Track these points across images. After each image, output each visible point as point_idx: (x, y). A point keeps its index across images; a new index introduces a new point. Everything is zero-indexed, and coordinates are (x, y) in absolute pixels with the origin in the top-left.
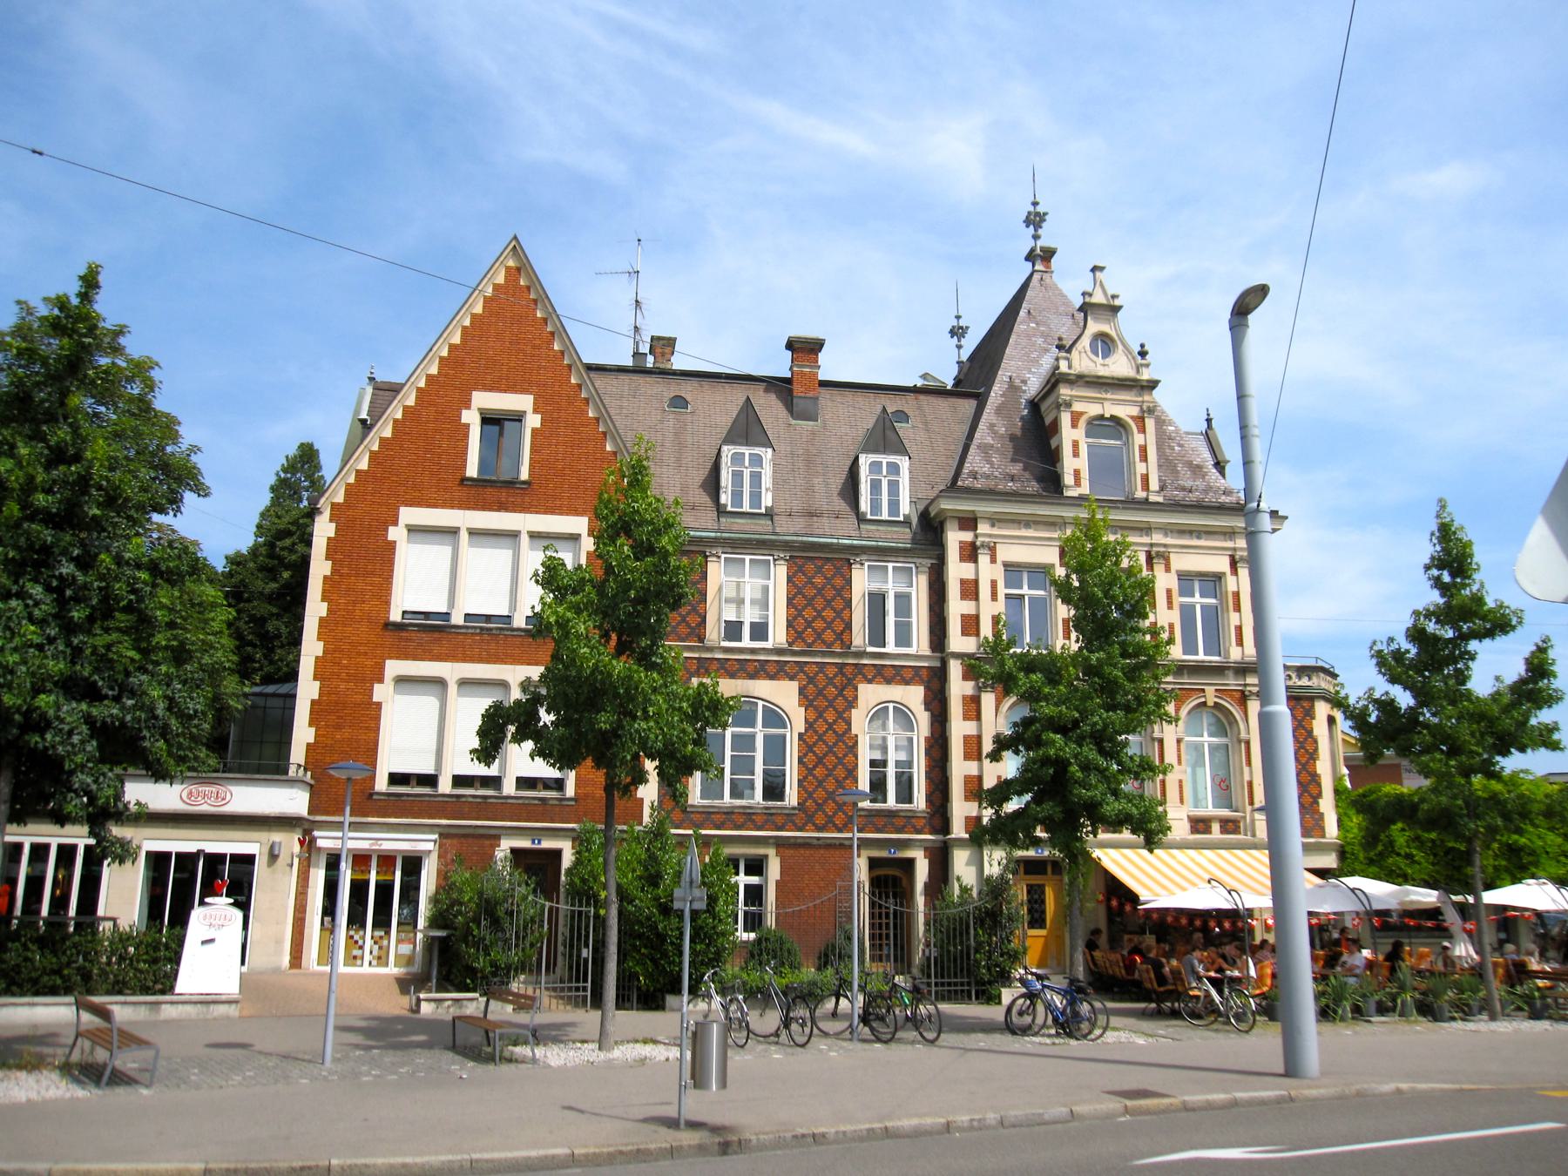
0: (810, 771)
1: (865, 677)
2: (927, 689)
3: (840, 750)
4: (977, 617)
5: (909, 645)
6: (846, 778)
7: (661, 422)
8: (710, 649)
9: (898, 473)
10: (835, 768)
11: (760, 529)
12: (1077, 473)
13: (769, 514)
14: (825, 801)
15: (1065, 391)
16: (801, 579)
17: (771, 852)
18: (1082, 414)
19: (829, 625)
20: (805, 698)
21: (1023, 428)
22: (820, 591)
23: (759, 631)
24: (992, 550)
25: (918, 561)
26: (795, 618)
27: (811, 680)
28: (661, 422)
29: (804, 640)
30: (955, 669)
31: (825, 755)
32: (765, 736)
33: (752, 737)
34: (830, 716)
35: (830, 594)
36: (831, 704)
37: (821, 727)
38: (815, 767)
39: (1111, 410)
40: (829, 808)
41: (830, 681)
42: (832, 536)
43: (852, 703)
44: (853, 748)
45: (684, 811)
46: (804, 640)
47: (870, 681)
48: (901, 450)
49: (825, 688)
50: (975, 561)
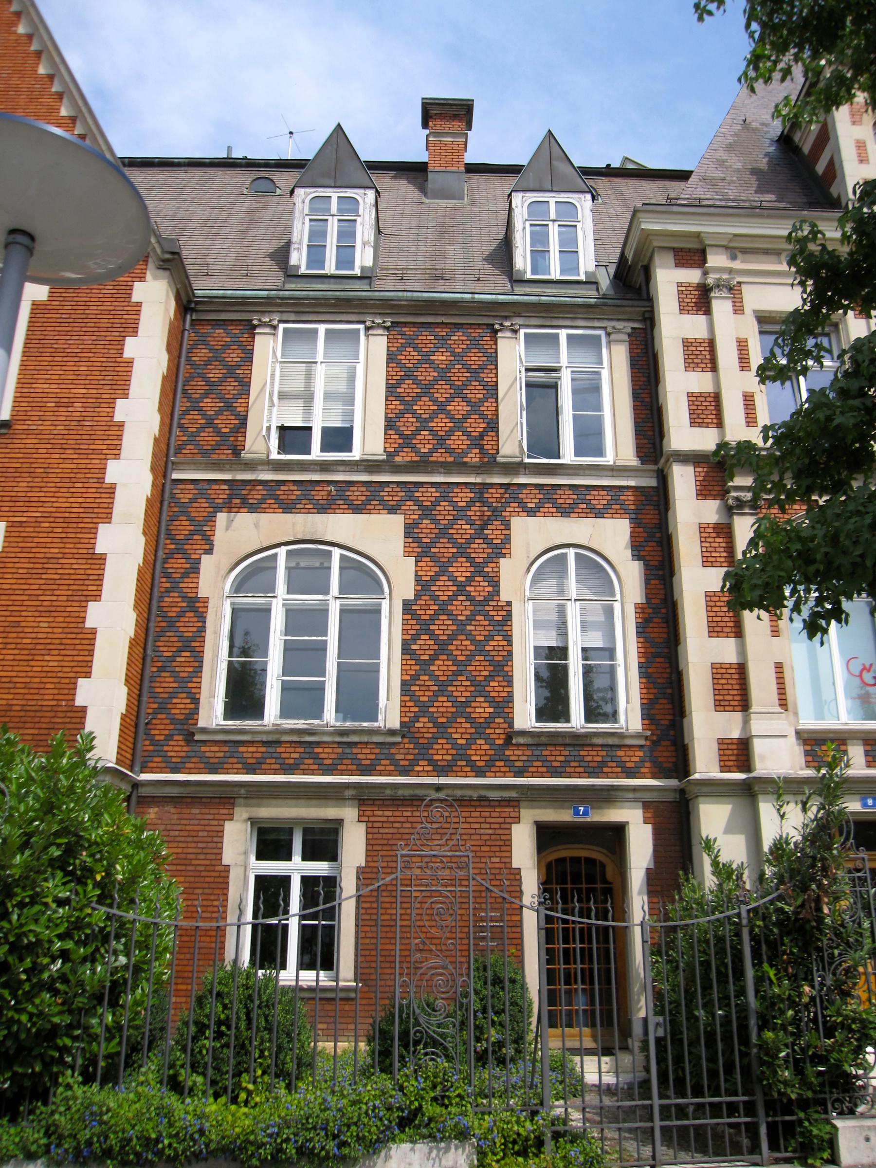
0: (424, 666)
2: (637, 524)
3: (479, 628)
4: (717, 398)
5: (599, 451)
6: (490, 678)
8: (251, 465)
10: (470, 658)
13: (366, 277)
14: (452, 719)
21: (769, 163)
22: (443, 373)
23: (338, 438)
24: (734, 291)
25: (609, 324)
26: (400, 415)
27: (427, 512)
30: (683, 481)
31: (452, 638)
36: (463, 551)
37: (444, 589)
38: (433, 659)
40: (460, 732)
44: (503, 623)
45: (189, 737)
47: (531, 513)
49: (451, 525)
50: (708, 312)
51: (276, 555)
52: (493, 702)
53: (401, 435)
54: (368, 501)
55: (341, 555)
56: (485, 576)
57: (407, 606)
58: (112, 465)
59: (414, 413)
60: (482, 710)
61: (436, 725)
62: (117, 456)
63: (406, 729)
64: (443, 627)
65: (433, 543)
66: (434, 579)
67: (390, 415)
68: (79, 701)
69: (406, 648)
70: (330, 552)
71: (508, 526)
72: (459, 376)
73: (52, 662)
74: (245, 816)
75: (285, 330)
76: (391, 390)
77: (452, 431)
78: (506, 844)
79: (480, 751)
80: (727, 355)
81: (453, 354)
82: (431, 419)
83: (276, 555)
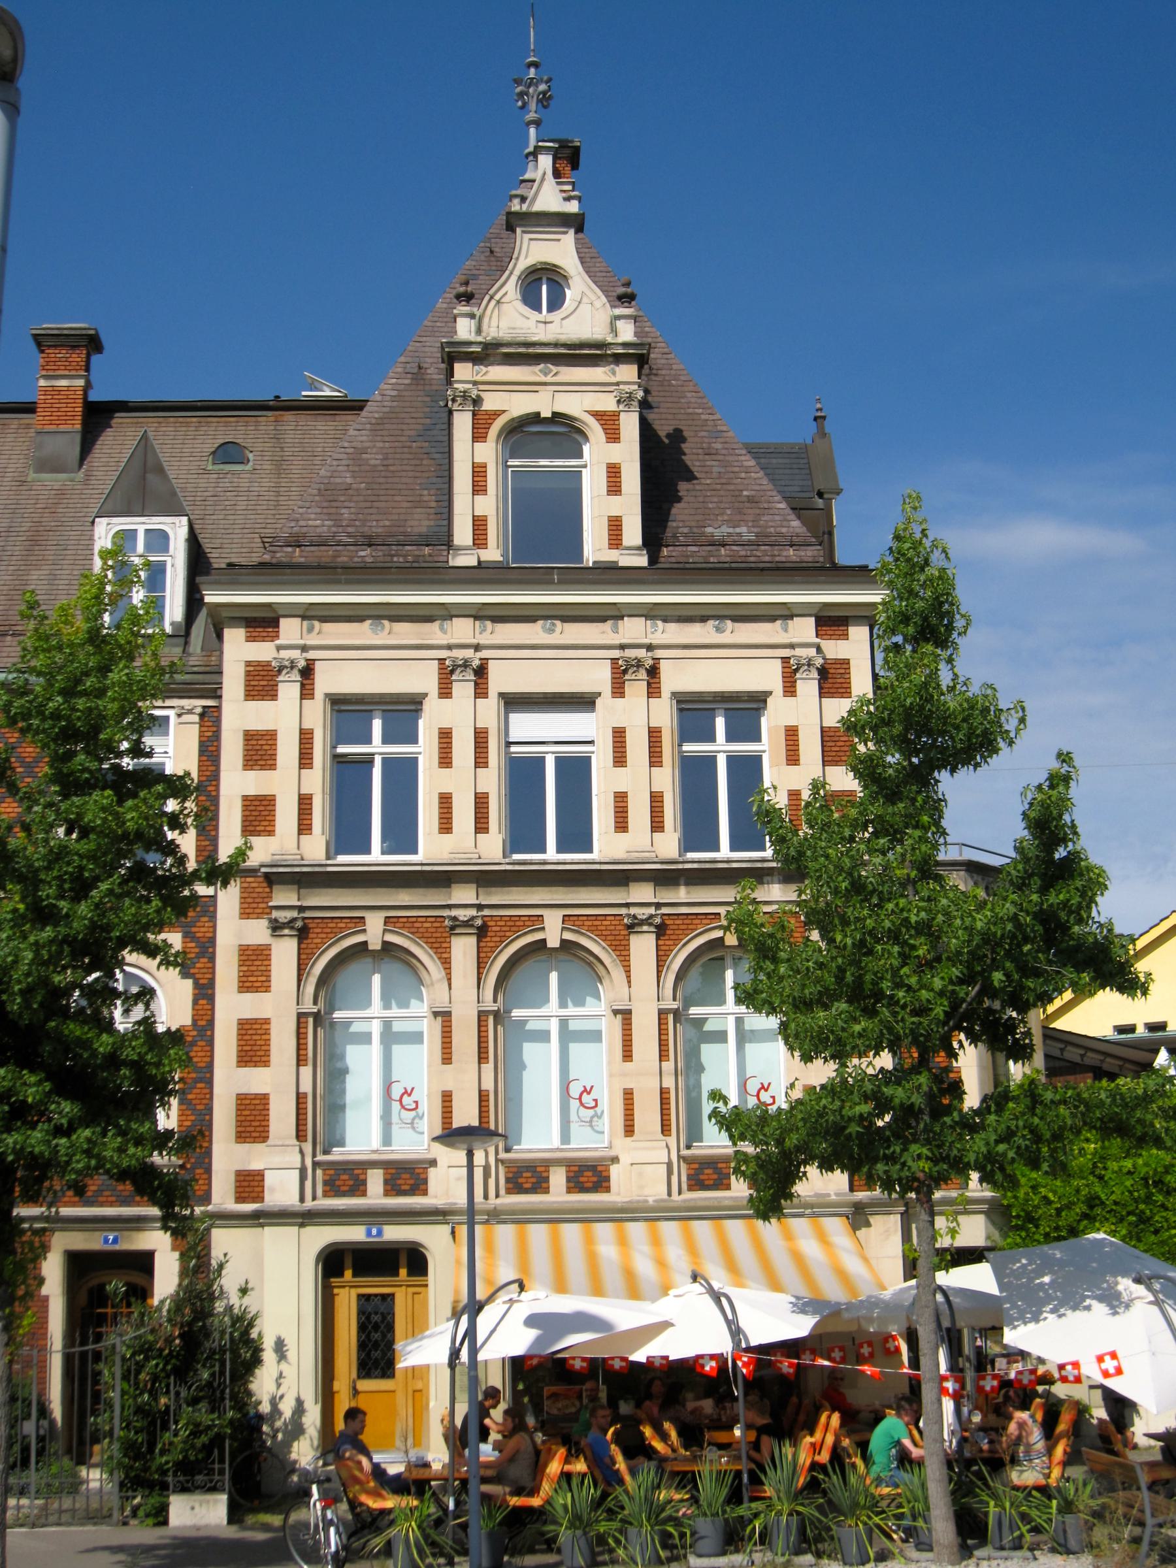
9: (165, 549)
12: (479, 524)
18: (497, 414)
39: (543, 404)
48: (174, 510)
80: (287, 750)
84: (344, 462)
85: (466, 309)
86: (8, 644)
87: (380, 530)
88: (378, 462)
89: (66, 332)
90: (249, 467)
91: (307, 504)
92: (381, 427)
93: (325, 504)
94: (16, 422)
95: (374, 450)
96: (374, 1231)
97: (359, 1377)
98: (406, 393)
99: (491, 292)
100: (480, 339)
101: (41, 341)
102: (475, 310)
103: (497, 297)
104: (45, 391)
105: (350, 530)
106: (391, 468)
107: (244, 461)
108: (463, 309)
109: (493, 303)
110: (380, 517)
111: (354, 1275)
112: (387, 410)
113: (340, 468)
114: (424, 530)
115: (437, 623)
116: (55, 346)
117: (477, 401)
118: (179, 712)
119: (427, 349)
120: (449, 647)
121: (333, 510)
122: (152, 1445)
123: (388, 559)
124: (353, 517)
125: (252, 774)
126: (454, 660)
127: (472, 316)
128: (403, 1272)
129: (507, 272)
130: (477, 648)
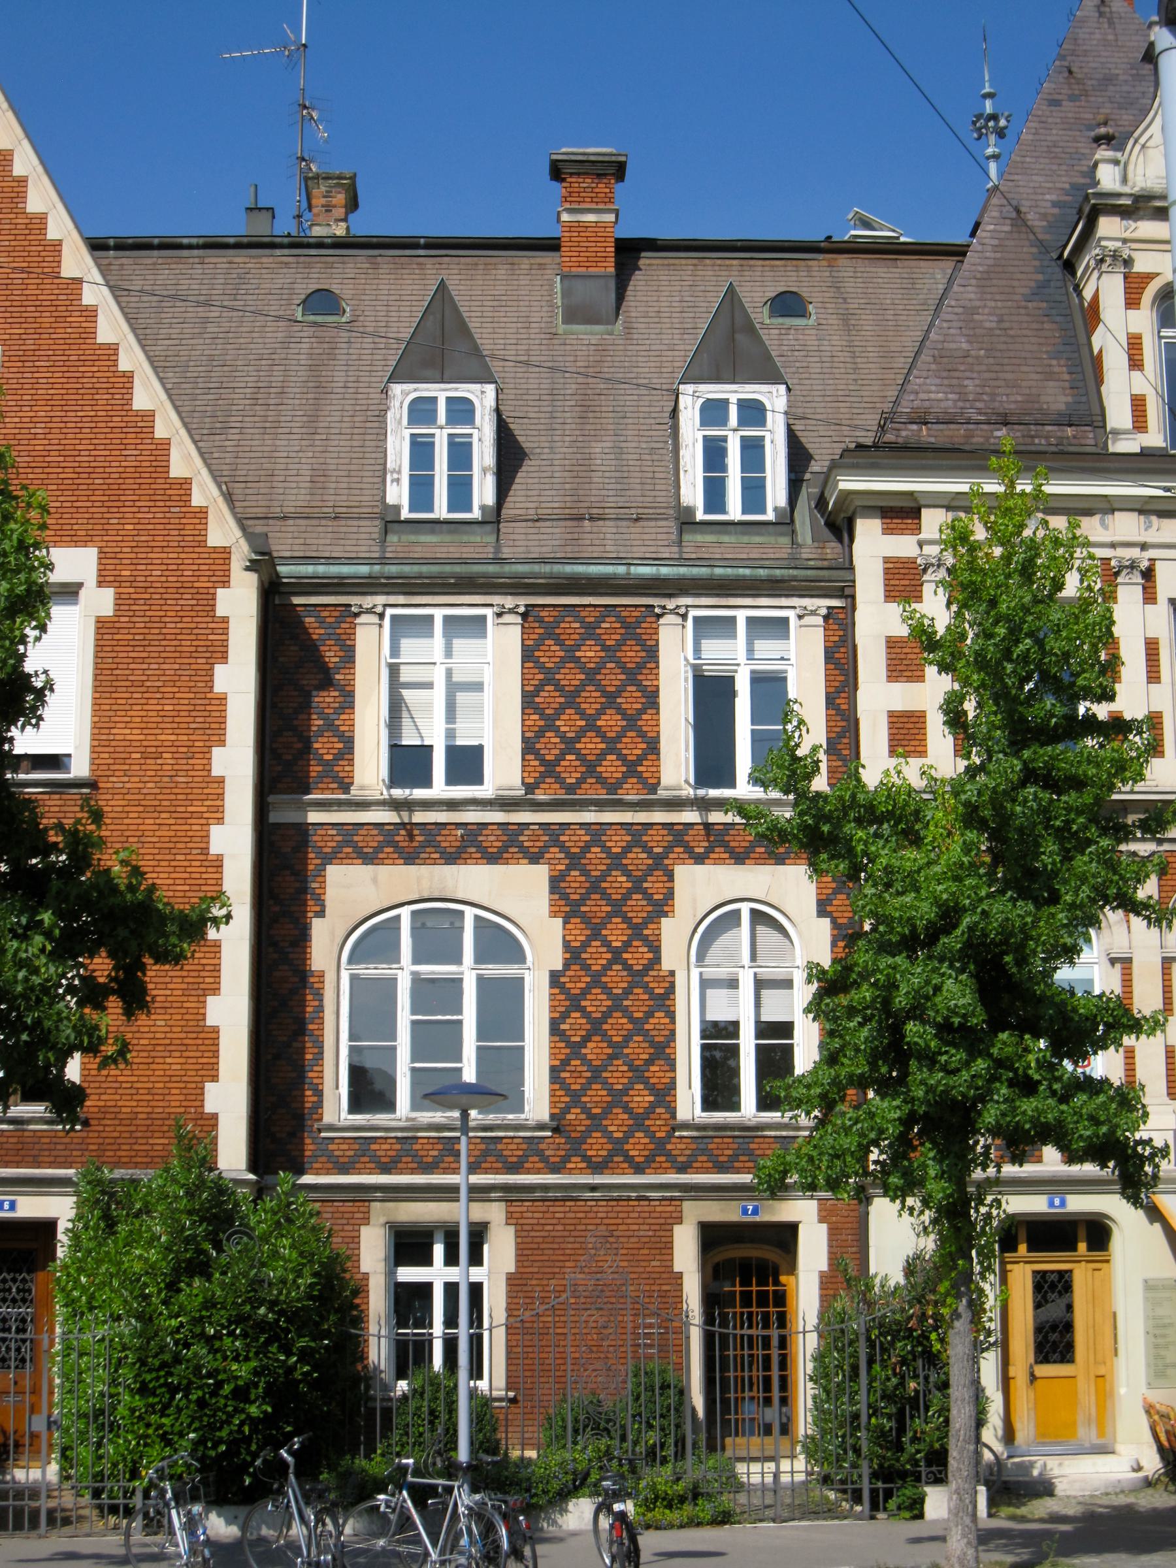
0: (576, 1049)
1: (689, 850)
3: (638, 1003)
6: (650, 1062)
7: (286, 345)
10: (627, 1039)
11: (467, 553)
12: (1138, 404)
14: (607, 1110)
15: (1108, 227)
16: (551, 653)
17: (494, 1213)
18: (1150, 277)
19: (612, 745)
20: (565, 902)
22: (592, 675)
23: (466, 763)
26: (540, 733)
27: (575, 860)
28: (286, 345)
29: (560, 780)
31: (607, 1015)
32: (480, 979)
33: (456, 983)
34: (616, 934)
35: (612, 678)
36: (618, 909)
37: (597, 956)
38: (586, 1039)
40: (617, 1124)
41: (616, 861)
42: (618, 560)
43: (663, 906)
44: (664, 999)
46: (560, 780)
47: (700, 859)
48: (771, 376)
49: (603, 877)
51: (398, 917)
52: (653, 1089)
53: (543, 762)
54: (504, 849)
55: (477, 917)
56: (645, 940)
57: (555, 977)
58: (215, 830)
59: (557, 730)
60: (641, 1099)
61: (591, 1116)
62: (220, 821)
63: (557, 1126)
64: (596, 1003)
65: (583, 900)
66: (585, 945)
67: (528, 735)
68: (209, 1108)
69: (555, 1028)
70: (462, 913)
71: (670, 877)
72: (612, 678)
73: (174, 1063)
74: (383, 1220)
75: (393, 617)
76: (529, 701)
77: (602, 755)
78: (666, 1247)
79: (638, 1146)
81: (605, 648)
82: (577, 739)
83: (398, 917)
84: (955, 324)
85: (1109, 154)
86: (588, 529)
87: (1013, 406)
88: (994, 325)
89: (592, 158)
90: (812, 321)
91: (925, 374)
92: (988, 283)
93: (945, 374)
94: (526, 261)
95: (986, 311)
96: (1057, 1202)
97: (1036, 1362)
98: (1007, 243)
99: (1136, 135)
100: (1126, 190)
101: (557, 171)
102: (1119, 154)
103: (1142, 141)
104: (570, 226)
105: (979, 405)
106: (1011, 332)
107: (804, 314)
108: (1103, 153)
109: (1138, 147)
110: (1008, 391)
111: (1029, 1251)
112: (991, 262)
113: (952, 331)
114: (1062, 407)
115: (1097, 517)
116: (579, 174)
117: (1128, 262)
118: (801, 612)
119: (1021, 190)
120: (1113, 545)
121: (955, 382)
122: (901, 1430)
123: (1029, 440)
124: (979, 390)
125: (897, 687)
126: (1120, 559)
127: (1116, 162)
128: (1082, 1246)
129: (1152, 113)
130: (1144, 546)
